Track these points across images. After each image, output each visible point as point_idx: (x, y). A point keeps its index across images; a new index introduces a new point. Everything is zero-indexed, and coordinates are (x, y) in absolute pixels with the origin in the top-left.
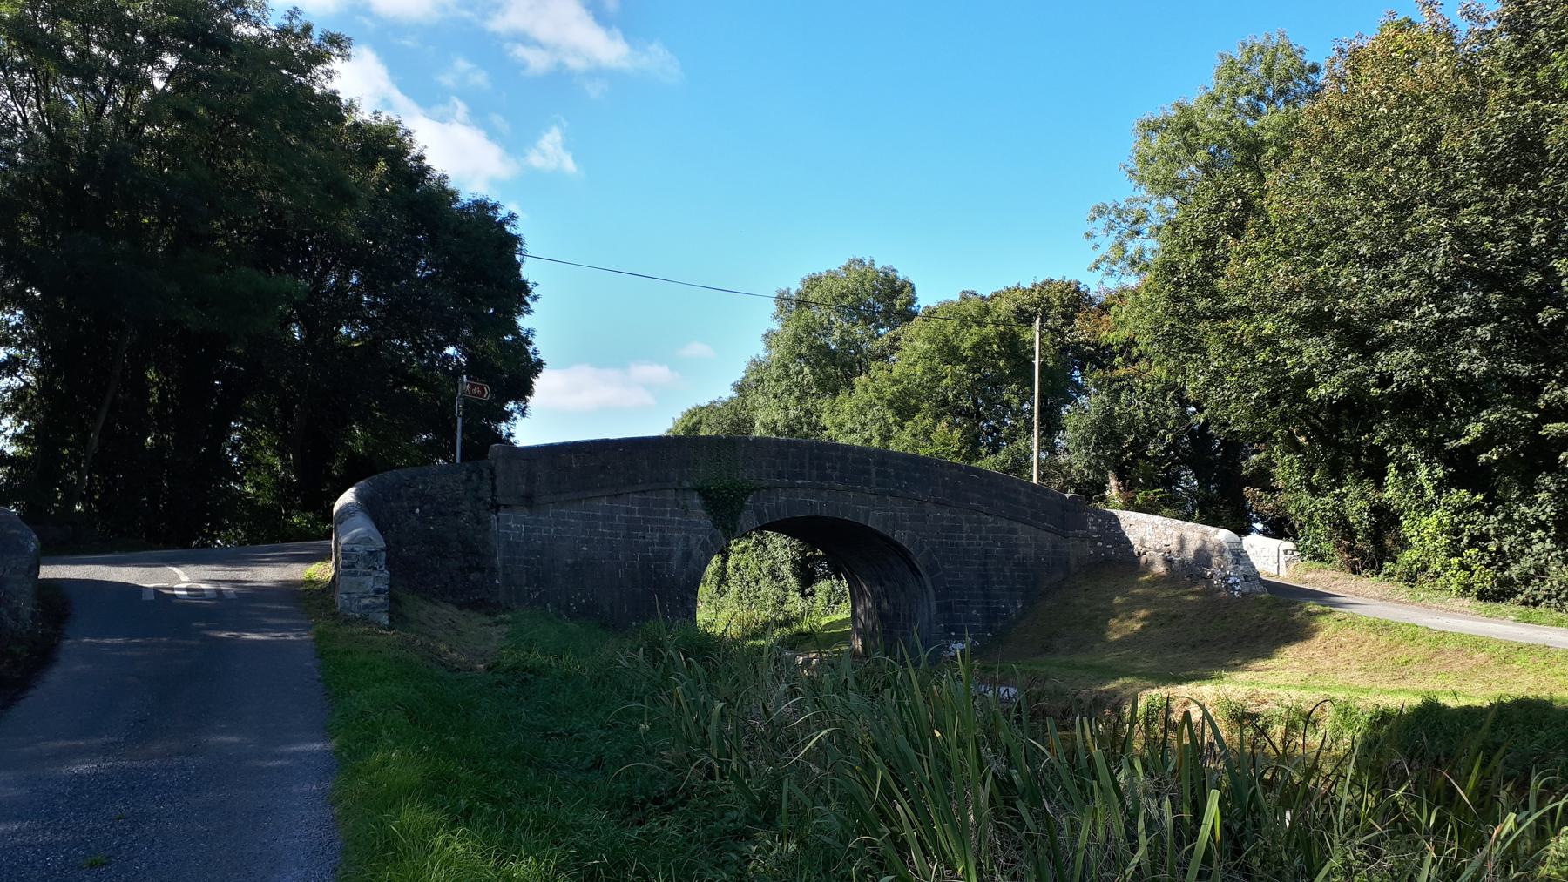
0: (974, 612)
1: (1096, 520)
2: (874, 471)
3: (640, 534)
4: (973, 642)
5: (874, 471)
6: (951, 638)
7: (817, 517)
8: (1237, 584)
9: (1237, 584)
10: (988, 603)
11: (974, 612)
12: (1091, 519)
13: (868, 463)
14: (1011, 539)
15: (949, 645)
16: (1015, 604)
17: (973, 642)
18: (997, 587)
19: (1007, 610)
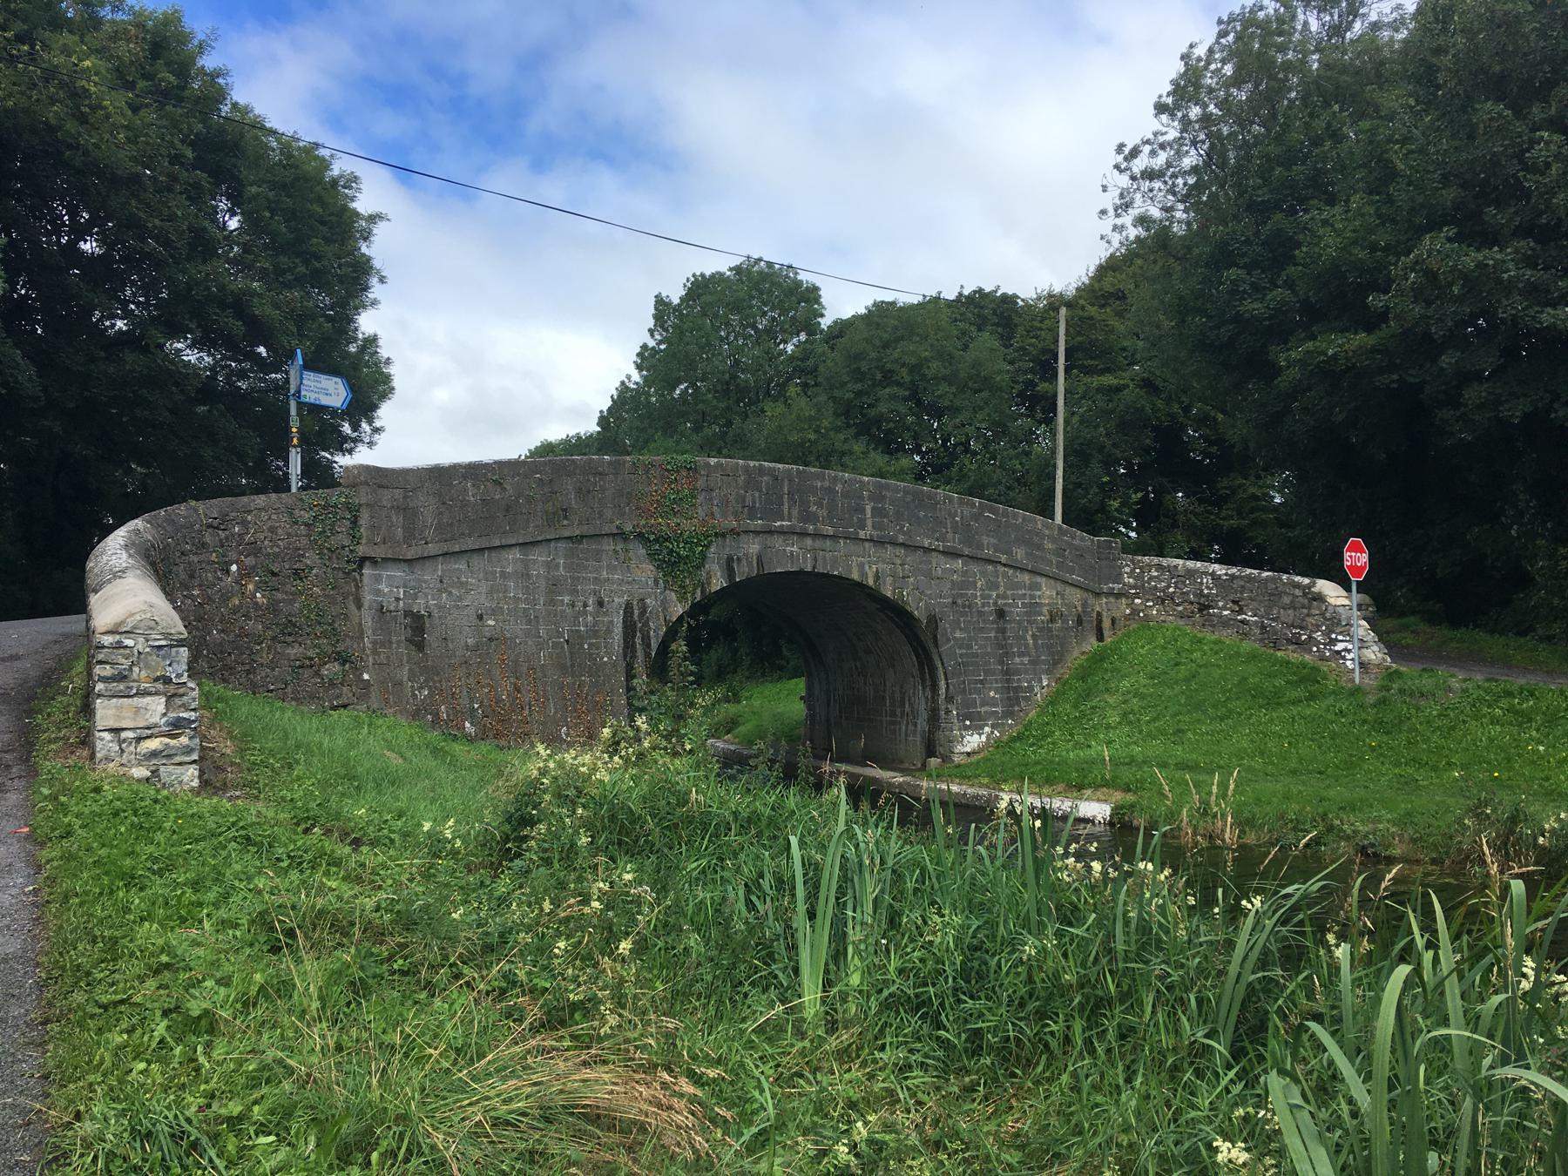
0: (992, 694)
1: (1133, 571)
2: (868, 509)
3: (567, 599)
4: (992, 733)
5: (868, 509)
6: (967, 728)
7: (801, 572)
8: (1349, 651)
9: (1349, 651)
10: (1008, 681)
11: (992, 694)
12: (1127, 569)
13: (861, 498)
14: (1032, 597)
15: (963, 737)
16: (1040, 681)
17: (992, 733)
18: (1017, 660)
19: (1030, 688)
